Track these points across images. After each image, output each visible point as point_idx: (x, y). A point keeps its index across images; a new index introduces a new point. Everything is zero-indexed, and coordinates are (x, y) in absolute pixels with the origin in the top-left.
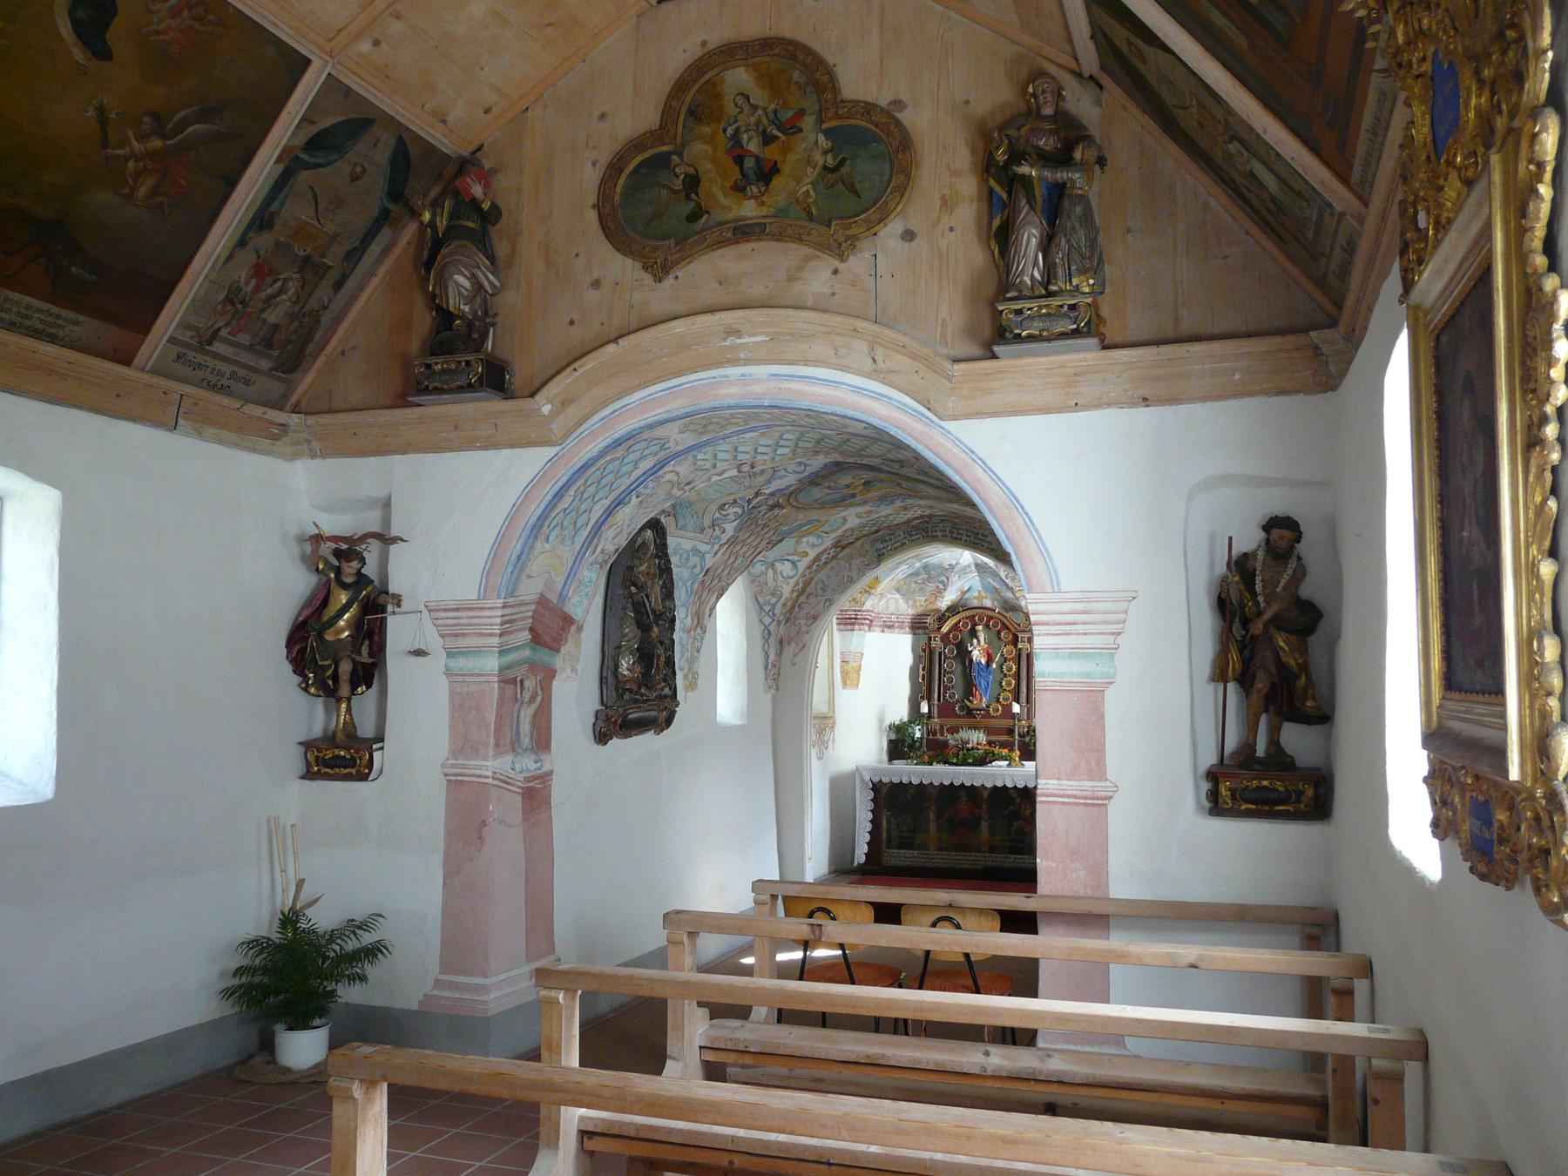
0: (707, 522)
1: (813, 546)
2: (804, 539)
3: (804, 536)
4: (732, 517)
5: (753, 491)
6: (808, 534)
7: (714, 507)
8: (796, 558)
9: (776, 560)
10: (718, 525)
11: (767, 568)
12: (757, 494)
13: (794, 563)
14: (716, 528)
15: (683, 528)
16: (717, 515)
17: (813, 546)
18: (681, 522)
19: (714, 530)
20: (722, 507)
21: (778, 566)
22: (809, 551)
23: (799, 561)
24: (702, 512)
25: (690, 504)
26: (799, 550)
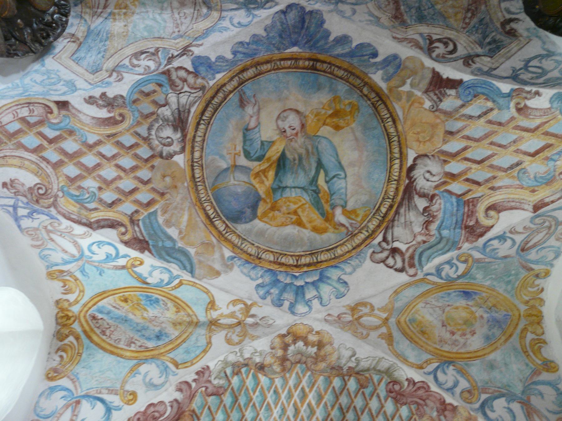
0: (110, 64)
1: (152, 386)
2: (143, 368)
3: (145, 360)
4: (141, 70)
5: (182, 43)
6: (153, 358)
7: (130, 51)
8: (114, 400)
9: (87, 396)
10: (119, 72)
11: (67, 406)
12: (185, 51)
13: (109, 410)
14: (115, 75)
15: (77, 61)
16: (126, 62)
17: (152, 386)
18: (81, 54)
19: (110, 76)
20: (137, 55)
21: (85, 405)
22: (140, 392)
23: (118, 409)
24: (112, 51)
25: (109, 36)
26: (128, 387)
